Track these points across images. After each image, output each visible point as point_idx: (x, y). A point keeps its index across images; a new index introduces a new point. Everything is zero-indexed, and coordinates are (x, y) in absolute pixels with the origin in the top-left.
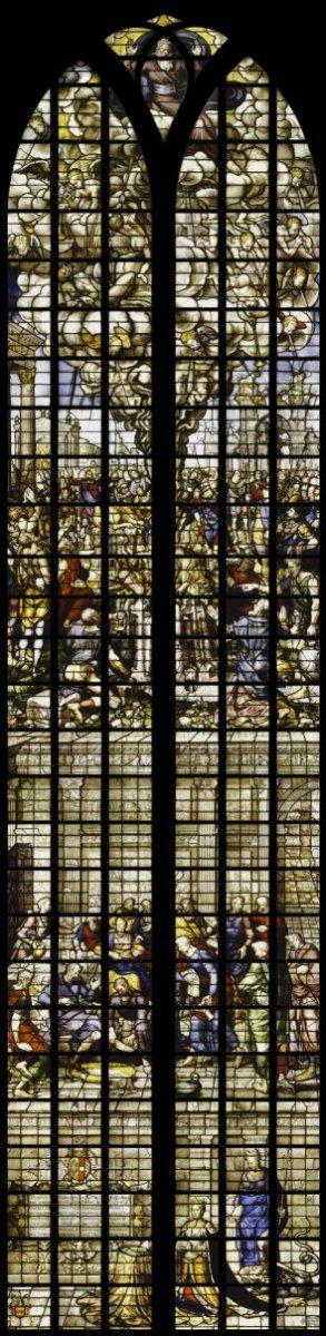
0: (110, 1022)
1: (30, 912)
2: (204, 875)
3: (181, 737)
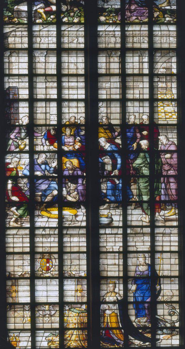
0: (64, 185)
1: (17, 124)
2: (113, 104)
3: (100, 28)
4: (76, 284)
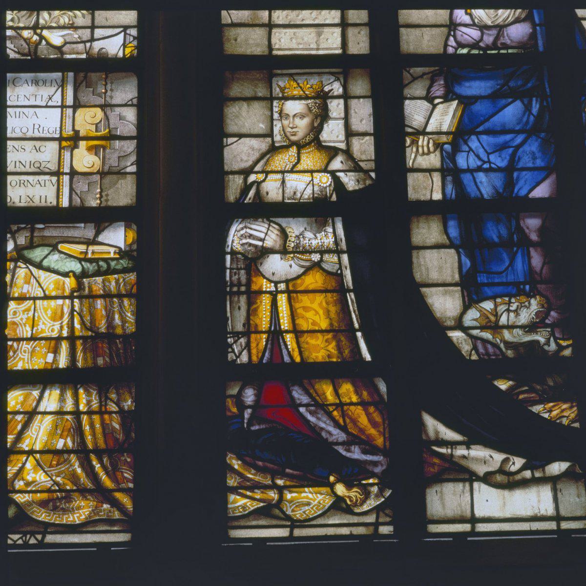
4: (70, 101)
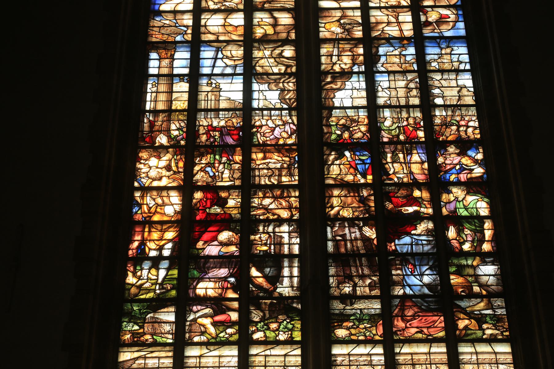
3: (337, 350)
